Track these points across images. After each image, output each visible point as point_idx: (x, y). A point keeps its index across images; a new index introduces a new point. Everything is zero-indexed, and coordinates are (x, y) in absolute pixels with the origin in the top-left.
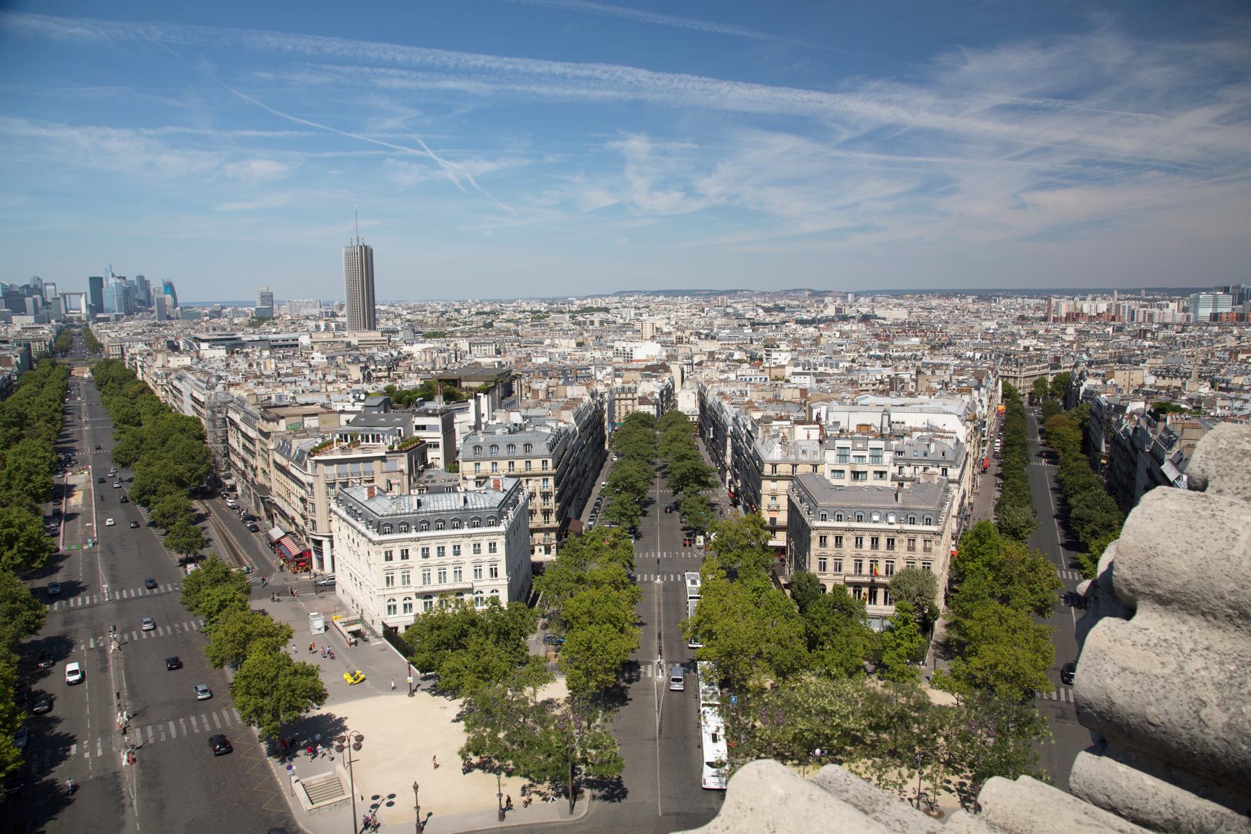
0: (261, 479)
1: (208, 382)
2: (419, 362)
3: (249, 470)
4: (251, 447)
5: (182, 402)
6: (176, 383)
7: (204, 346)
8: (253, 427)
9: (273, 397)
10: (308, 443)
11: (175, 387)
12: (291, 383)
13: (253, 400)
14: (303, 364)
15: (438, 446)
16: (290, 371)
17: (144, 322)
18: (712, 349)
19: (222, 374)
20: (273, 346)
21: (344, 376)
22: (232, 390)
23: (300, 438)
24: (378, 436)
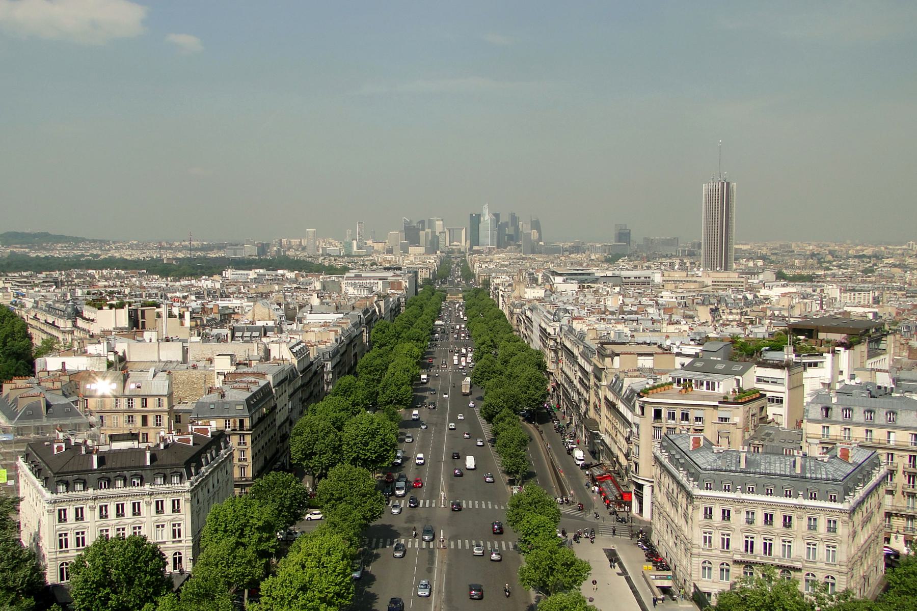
1: (555, 315)
3: (583, 405)
5: (532, 331)
6: (528, 313)
8: (590, 362)
9: (612, 333)
11: (527, 317)
12: (633, 320)
13: (591, 335)
14: (651, 302)
16: (634, 309)
17: (512, 255)
19: (569, 307)
21: (692, 317)
22: (575, 322)
23: (632, 377)
24: (713, 383)
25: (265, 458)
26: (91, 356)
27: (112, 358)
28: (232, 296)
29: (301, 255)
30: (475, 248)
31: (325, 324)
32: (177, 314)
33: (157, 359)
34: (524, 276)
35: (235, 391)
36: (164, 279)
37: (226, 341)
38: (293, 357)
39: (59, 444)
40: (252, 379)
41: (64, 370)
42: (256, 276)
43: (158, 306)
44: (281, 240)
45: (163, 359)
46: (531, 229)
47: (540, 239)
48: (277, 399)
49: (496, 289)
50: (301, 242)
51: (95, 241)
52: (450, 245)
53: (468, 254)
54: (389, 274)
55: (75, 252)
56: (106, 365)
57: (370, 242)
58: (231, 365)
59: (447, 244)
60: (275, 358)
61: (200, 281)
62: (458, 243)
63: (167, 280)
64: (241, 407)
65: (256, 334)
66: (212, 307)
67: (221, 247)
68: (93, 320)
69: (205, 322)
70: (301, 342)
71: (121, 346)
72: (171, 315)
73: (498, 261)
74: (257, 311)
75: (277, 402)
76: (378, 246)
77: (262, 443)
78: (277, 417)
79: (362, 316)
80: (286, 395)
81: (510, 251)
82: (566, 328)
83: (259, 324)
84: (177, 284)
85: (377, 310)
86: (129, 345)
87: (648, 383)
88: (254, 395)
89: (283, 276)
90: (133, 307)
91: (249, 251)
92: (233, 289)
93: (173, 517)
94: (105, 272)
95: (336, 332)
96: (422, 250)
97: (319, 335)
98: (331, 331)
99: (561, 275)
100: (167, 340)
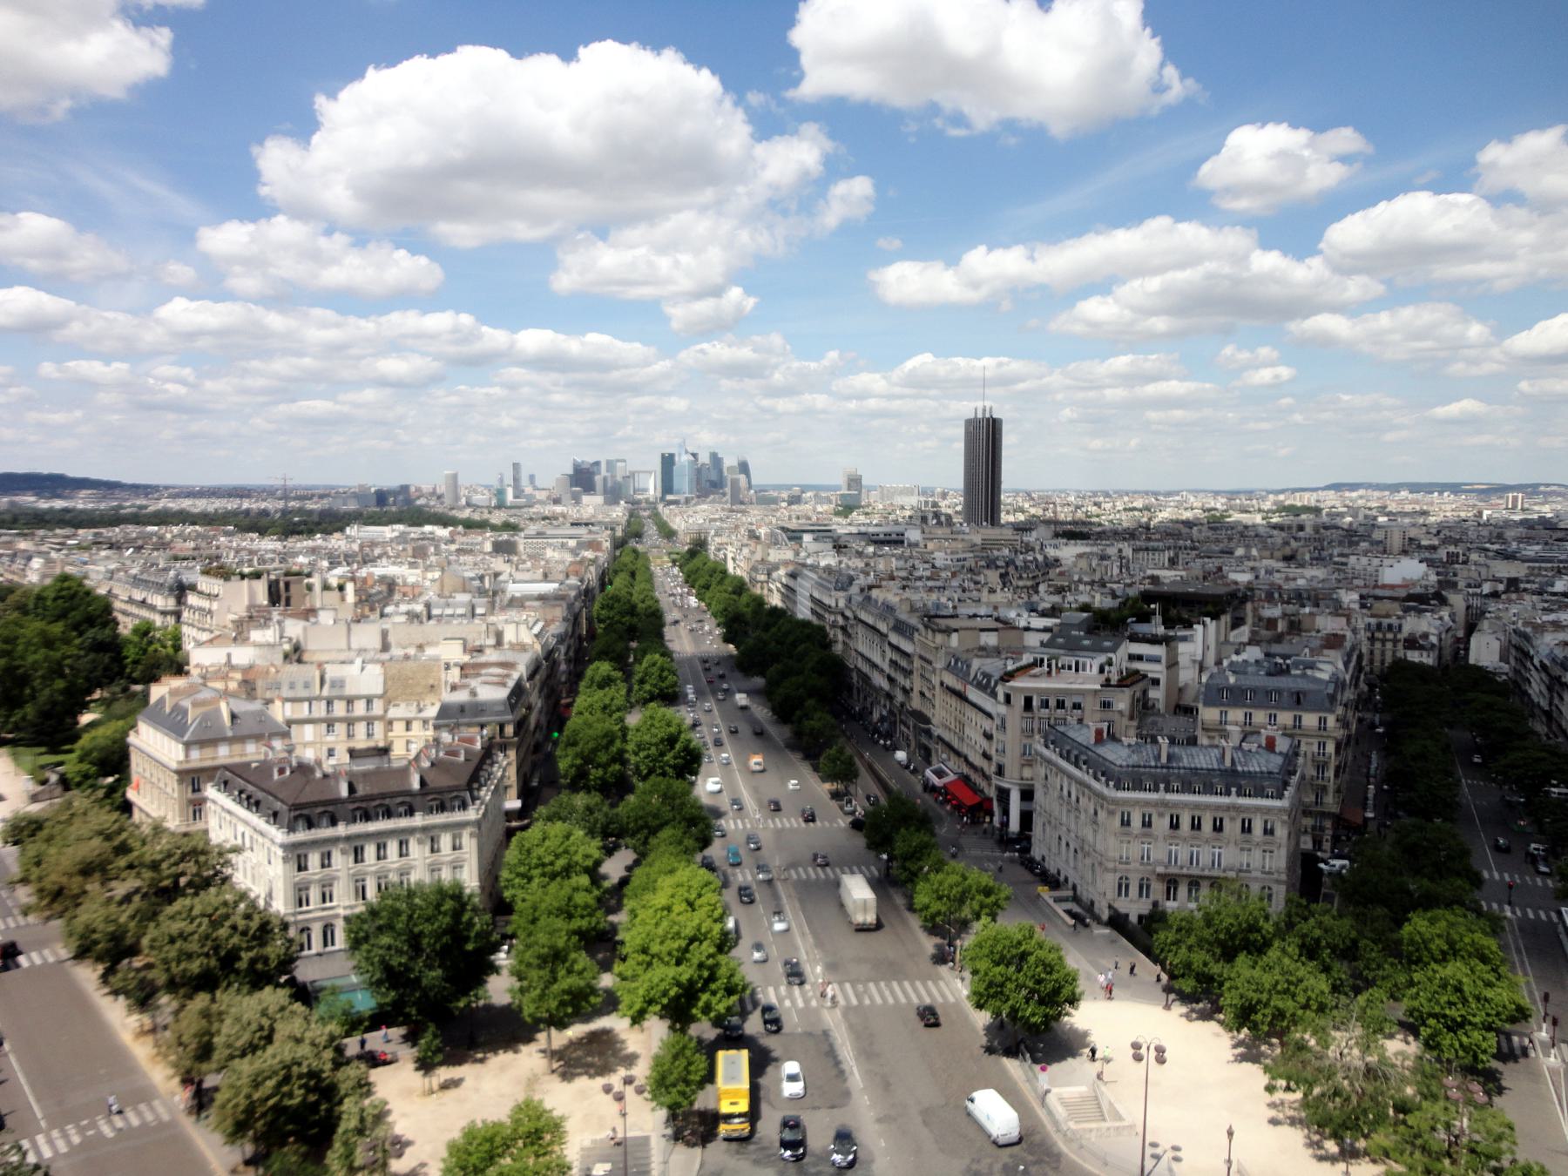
0: (916, 703)
10: (994, 666)
18: (1513, 574)
29: (439, 509)
43: (309, 575)
54: (582, 531)
58: (465, 651)
74: (447, 581)
82: (860, 599)
86: (305, 629)
89: (431, 533)
96: (598, 499)
99: (813, 531)
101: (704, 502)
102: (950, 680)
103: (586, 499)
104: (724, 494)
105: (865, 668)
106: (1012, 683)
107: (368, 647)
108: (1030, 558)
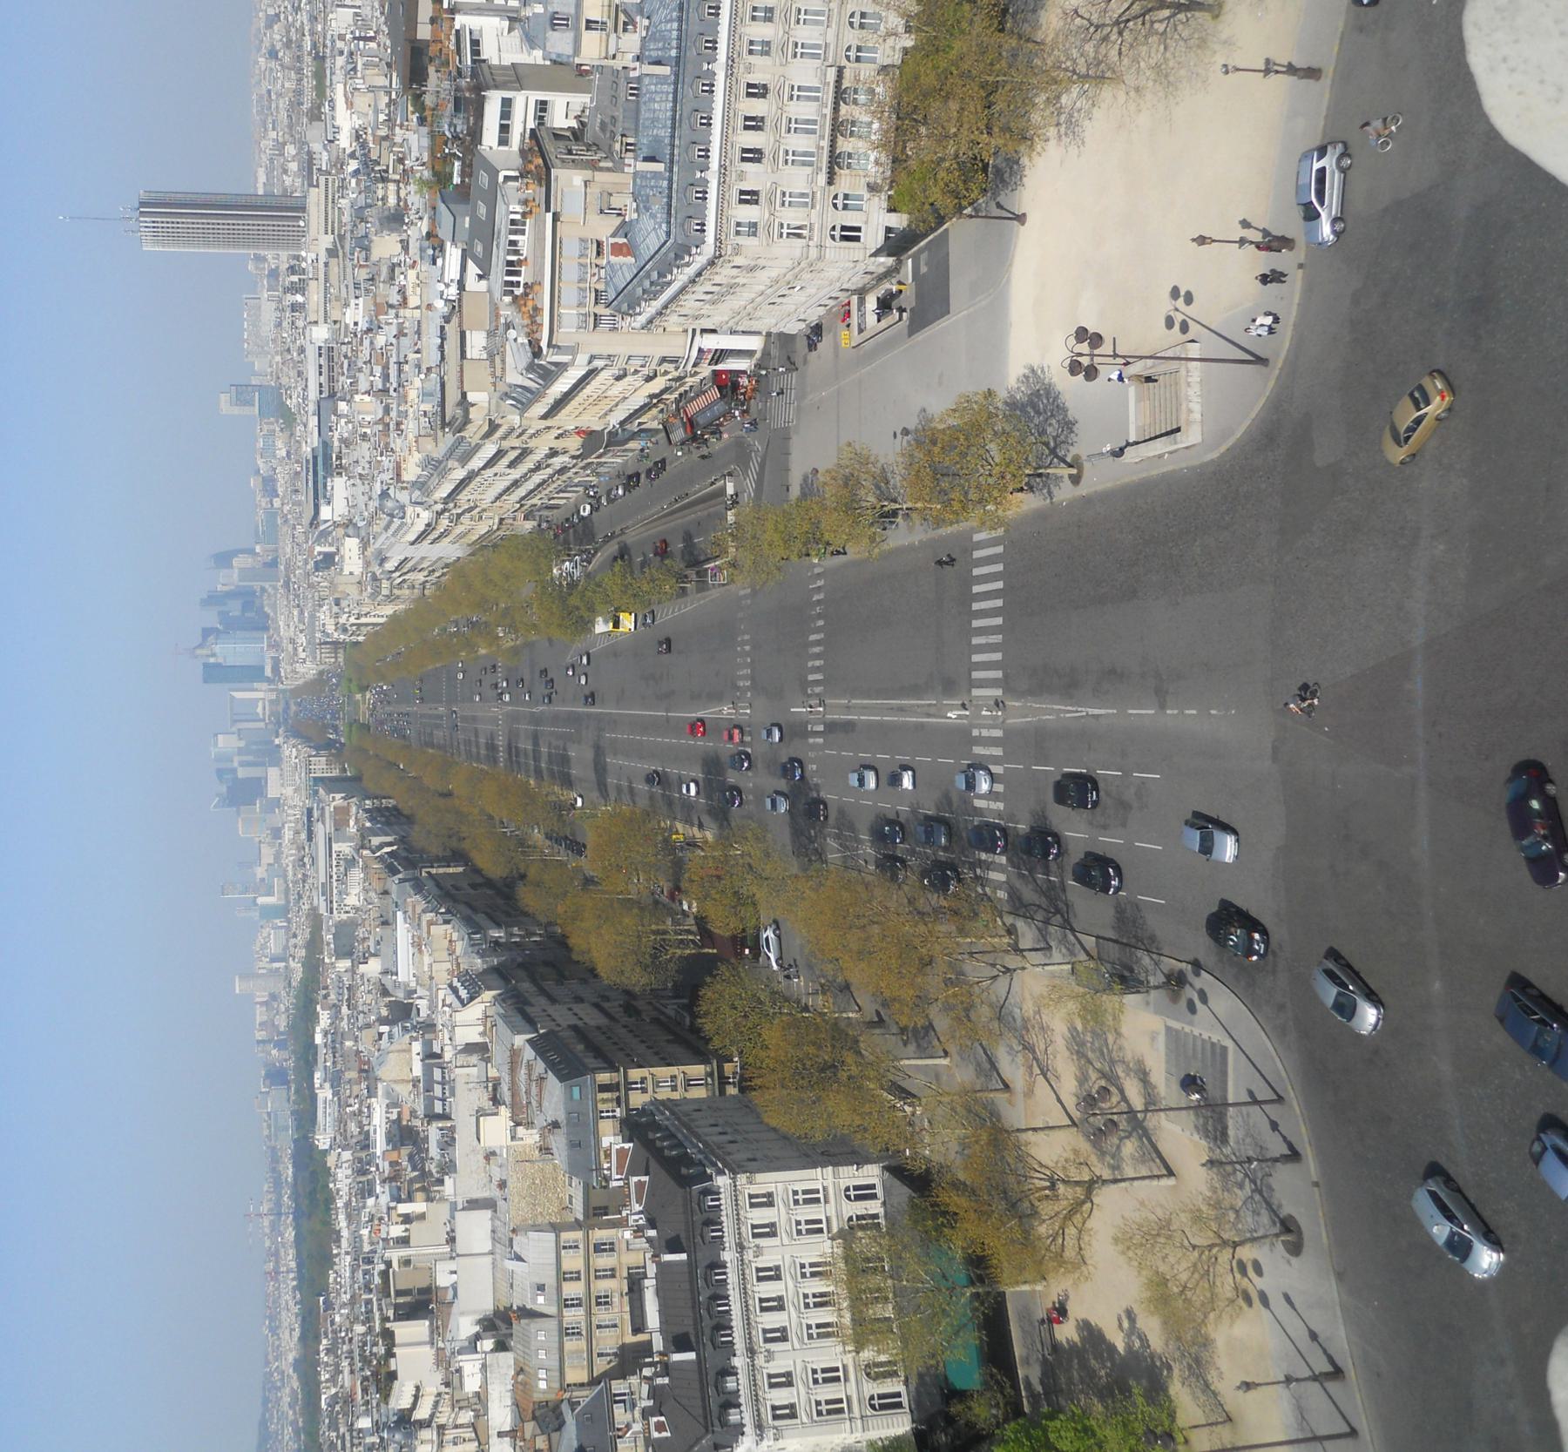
1: (392, 516)
2: (371, 117)
3: (558, 462)
4: (512, 455)
5: (423, 559)
6: (389, 566)
7: (325, 513)
8: (478, 447)
9: (423, 407)
11: (397, 569)
12: (400, 371)
15: (544, 103)
19: (378, 489)
20: (331, 396)
22: (406, 477)
23: (503, 369)
25: (668, 1041)
26: (485, 1383)
27: (488, 1344)
28: (366, 1128)
29: (287, 1002)
30: (268, 672)
31: (418, 945)
32: (403, 1227)
33: (489, 1259)
34: (319, 579)
35: (545, 1104)
36: (337, 1260)
37: (452, 1129)
38: (479, 999)
39: (652, 1428)
40: (523, 1072)
41: (512, 1434)
42: (327, 1085)
43: (389, 1264)
44: (259, 1042)
45: (488, 1246)
46: (231, 567)
47: (252, 552)
48: (559, 1025)
49: (345, 630)
50: (262, 1004)
51: (266, 1401)
52: (264, 720)
53: (281, 686)
54: (321, 831)
55: (287, 1438)
56: (502, 1355)
57: (260, 872)
58: (496, 1114)
59: (262, 725)
60: (483, 1034)
61: (338, 1190)
62: (260, 704)
63: (338, 1254)
64: (576, 1090)
65: (437, 1075)
66: (387, 1164)
67: (275, 1160)
68: (418, 1388)
69: (416, 1173)
70: (451, 986)
71: (464, 1326)
72: (404, 1241)
73: (292, 629)
74: (393, 1076)
75: (564, 1024)
76: (267, 855)
77: (642, 1048)
78: (592, 1023)
79: (400, 876)
80: (551, 1010)
81: (274, 607)
82: (417, 493)
83: (418, 1070)
84: (345, 1233)
85: (388, 849)
86: (462, 1314)
87: (515, 340)
88: (552, 1066)
89: (326, 1034)
90: (391, 1313)
91: (279, 1103)
92: (353, 1128)
93: (792, 1309)
94: (324, 1376)
95: (430, 923)
96: (273, 773)
97: (436, 955)
98: (429, 932)
100: (451, 1240)
101: (275, 621)
102: (540, 408)
103: (272, 792)
104: (263, 590)
105: (521, 492)
106: (544, 344)
107: (489, 1228)
108: (353, 181)
